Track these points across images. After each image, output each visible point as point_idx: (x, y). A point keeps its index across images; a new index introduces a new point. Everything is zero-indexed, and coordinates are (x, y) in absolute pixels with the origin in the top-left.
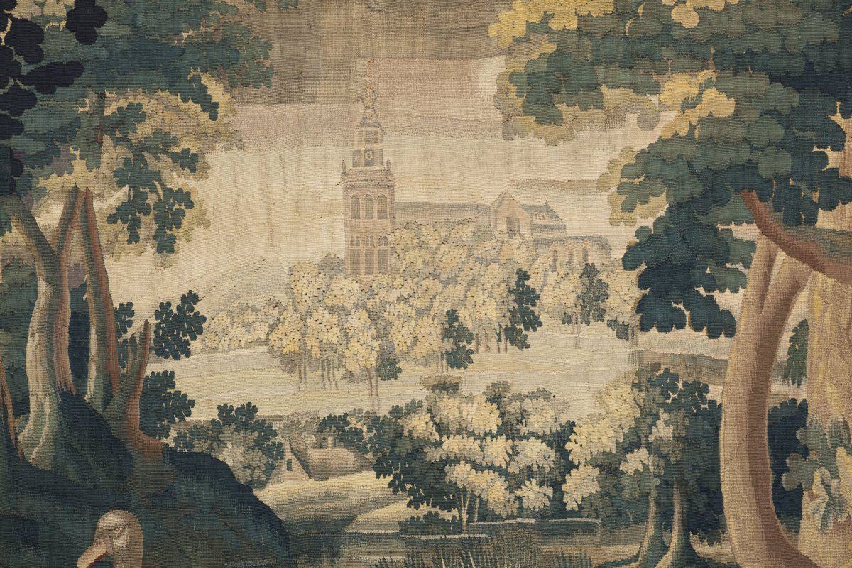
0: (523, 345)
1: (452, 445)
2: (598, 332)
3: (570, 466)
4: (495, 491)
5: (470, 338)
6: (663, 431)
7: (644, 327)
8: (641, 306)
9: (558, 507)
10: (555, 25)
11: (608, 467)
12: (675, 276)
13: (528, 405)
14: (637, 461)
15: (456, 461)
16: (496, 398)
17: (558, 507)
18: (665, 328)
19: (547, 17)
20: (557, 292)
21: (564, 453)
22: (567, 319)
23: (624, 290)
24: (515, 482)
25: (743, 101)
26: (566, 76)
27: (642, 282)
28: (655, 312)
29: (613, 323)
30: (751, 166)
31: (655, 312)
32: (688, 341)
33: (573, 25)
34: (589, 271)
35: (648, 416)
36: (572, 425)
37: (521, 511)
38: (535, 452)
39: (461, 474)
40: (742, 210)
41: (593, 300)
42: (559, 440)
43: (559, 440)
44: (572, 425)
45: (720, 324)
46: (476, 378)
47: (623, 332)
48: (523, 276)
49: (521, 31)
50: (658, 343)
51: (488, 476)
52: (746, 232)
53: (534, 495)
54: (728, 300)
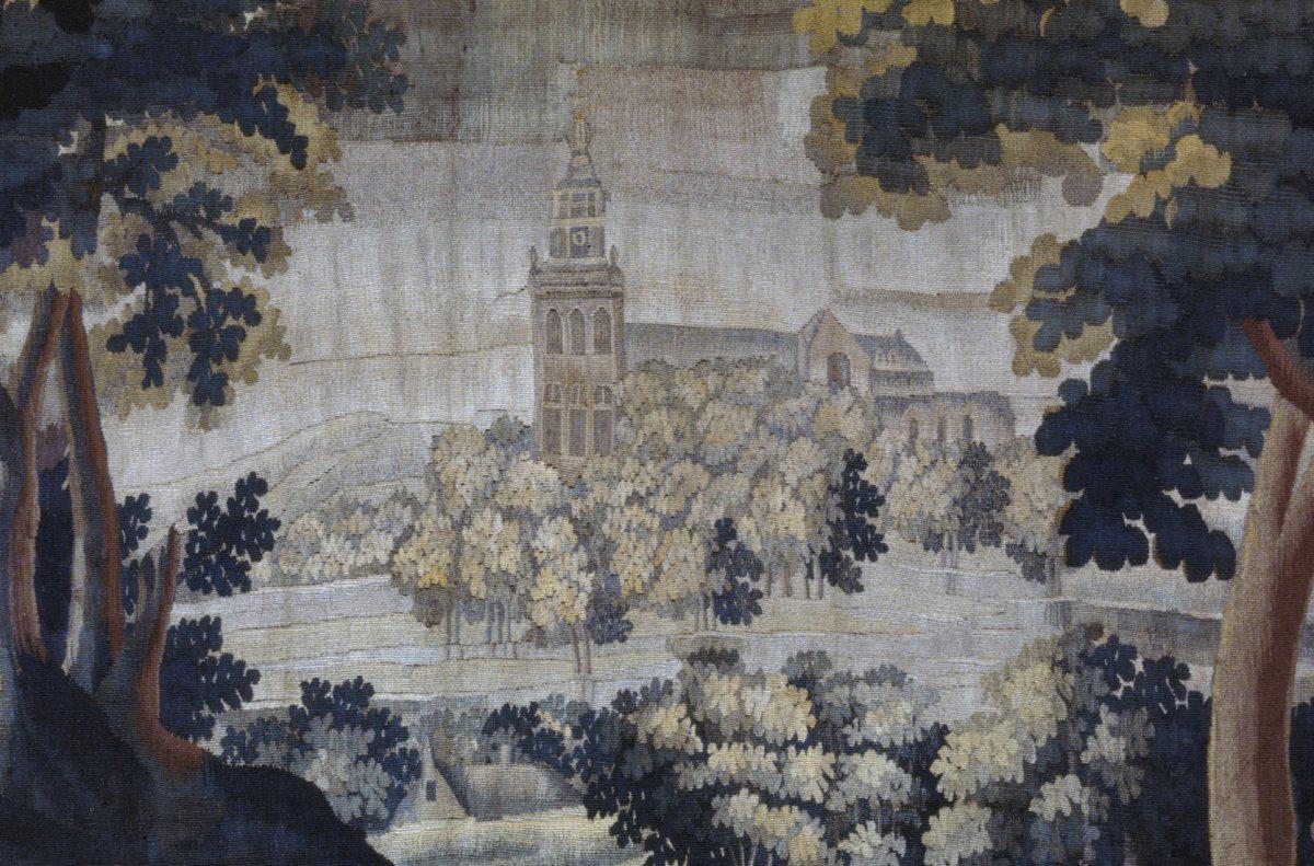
0: (852, 585)
1: (725, 760)
2: (989, 566)
3: (936, 803)
5: (756, 569)
6: (1107, 744)
7: (1074, 559)
8: (1069, 522)
10: (914, 17)
11: (1009, 805)
12: (1128, 467)
13: (864, 693)
14: (1061, 796)
15: (734, 788)
16: (806, 677)
18: (1110, 563)
20: (915, 489)
22: (933, 542)
23: (1039, 491)
25: (1246, 158)
26: (935, 103)
27: (1070, 479)
28: (1092, 533)
29: (1017, 551)
30: (1261, 275)
31: (1092, 533)
32: (1151, 586)
33: (947, 17)
34: (975, 457)
38: (874, 774)
39: (741, 810)
40: (1244, 353)
41: (980, 508)
42: (919, 756)
43: (919, 756)
45: (1205, 555)
47: (1035, 567)
48: (856, 463)
50: (1098, 589)
51: (790, 815)
52: (1254, 391)
54: (1225, 514)
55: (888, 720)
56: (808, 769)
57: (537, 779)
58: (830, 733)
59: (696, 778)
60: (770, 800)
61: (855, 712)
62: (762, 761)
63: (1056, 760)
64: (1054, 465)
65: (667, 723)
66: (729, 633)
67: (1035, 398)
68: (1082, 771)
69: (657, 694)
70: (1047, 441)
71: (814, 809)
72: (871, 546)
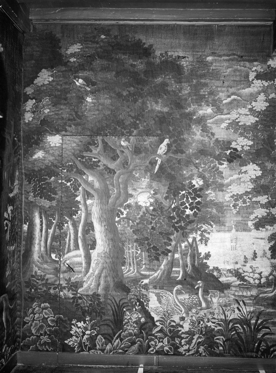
0: (255, 260)
1: (245, 274)
2: (265, 259)
3: (262, 278)
4: (252, 281)
5: (247, 259)
7: (272, 258)
9: (260, 283)
10: (258, 217)
11: (267, 278)
13: (255, 269)
14: (271, 277)
15: (246, 276)
16: (251, 267)
17: (260, 283)
19: (258, 216)
20: (259, 253)
21: (261, 276)
22: (261, 257)
24: (254, 280)
26: (260, 224)
27: (271, 253)
29: (267, 258)
33: (261, 217)
34: (264, 251)
35: (273, 271)
36: (262, 272)
37: (255, 284)
38: (257, 276)
39: (246, 278)
41: (265, 254)
42: (260, 274)
43: (260, 274)
44: (262, 272)
46: (248, 265)
47: (269, 259)
49: (254, 218)
51: (250, 278)
53: (257, 282)
55: (258, 271)
56: (251, 275)
57: (230, 275)
58: (253, 272)
59: (243, 275)
60: (249, 277)
61: (255, 270)
62: (248, 274)
63: (271, 274)
64: (270, 251)
65: (241, 271)
66: (245, 264)
67: (269, 246)
68: (273, 275)
69: (240, 268)
70: (269, 250)
71: (252, 278)
72: (256, 257)
